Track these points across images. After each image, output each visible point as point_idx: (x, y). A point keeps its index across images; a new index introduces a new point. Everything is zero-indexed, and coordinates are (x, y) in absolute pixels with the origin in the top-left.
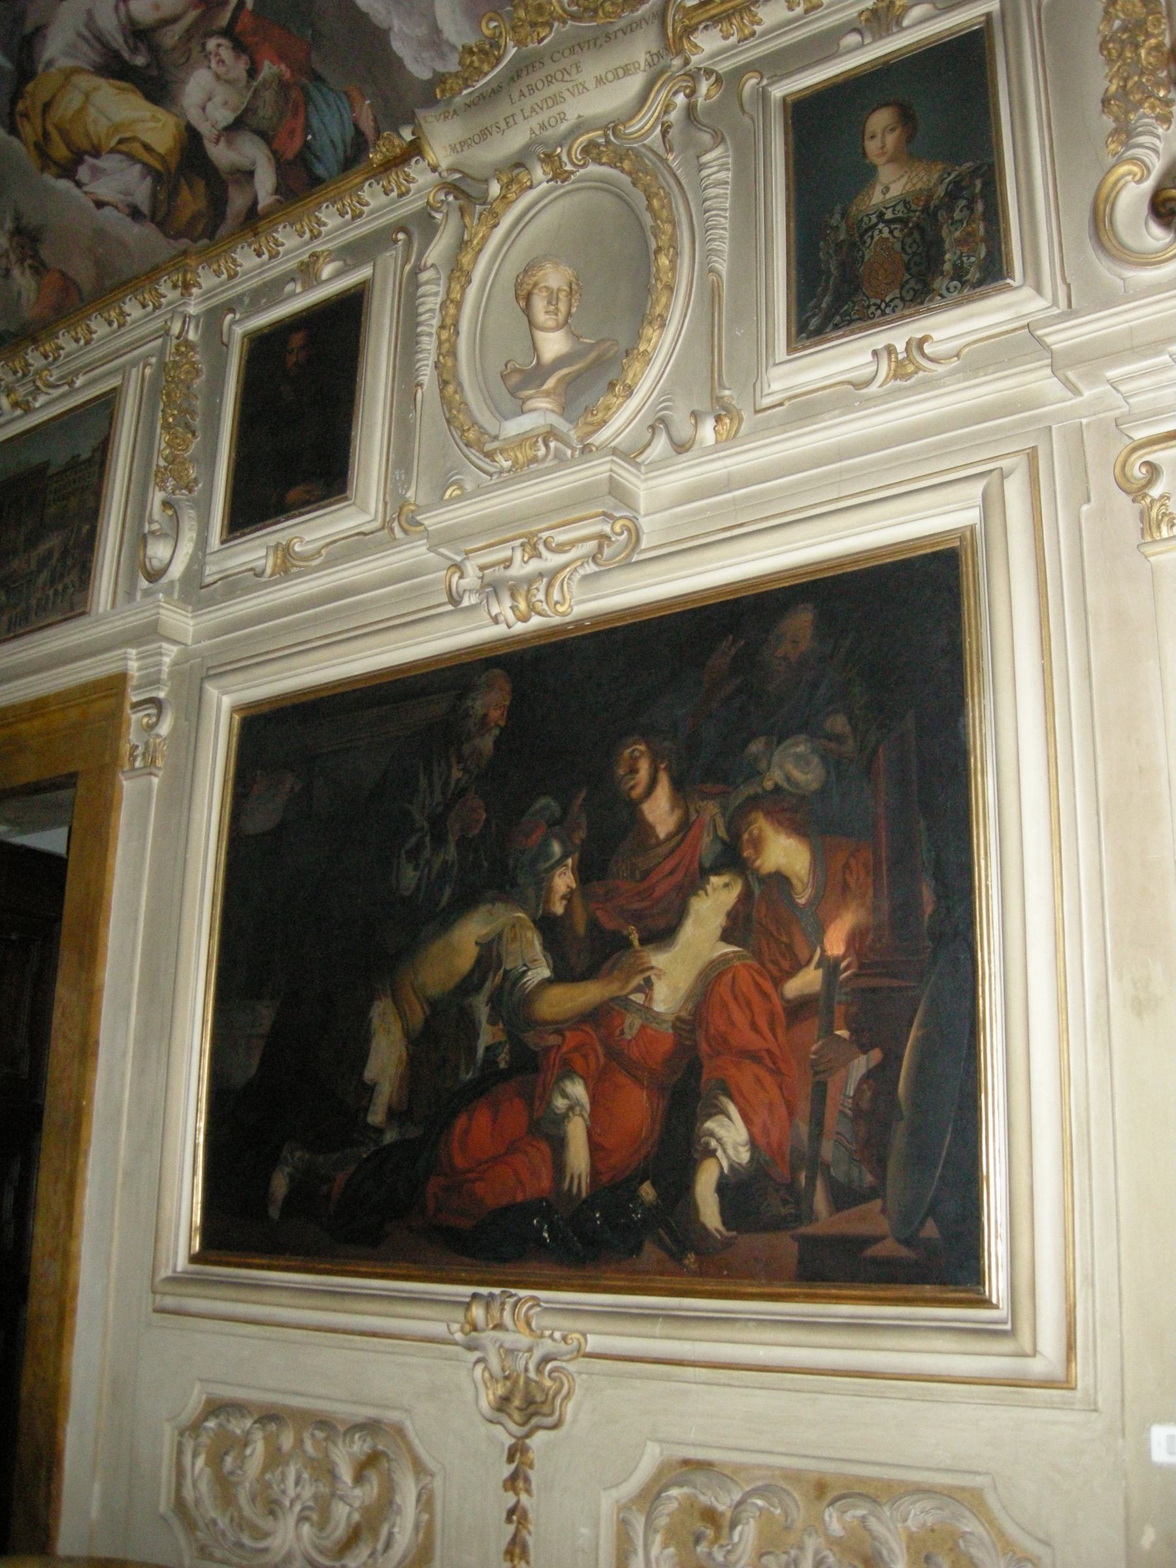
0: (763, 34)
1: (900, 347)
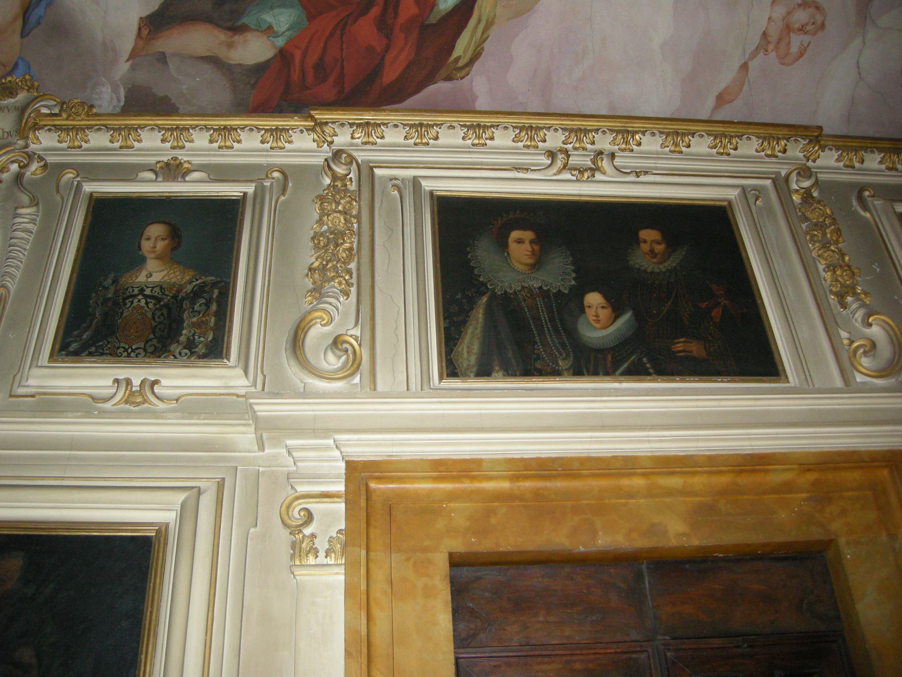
0: (86, 150)
1: (136, 382)
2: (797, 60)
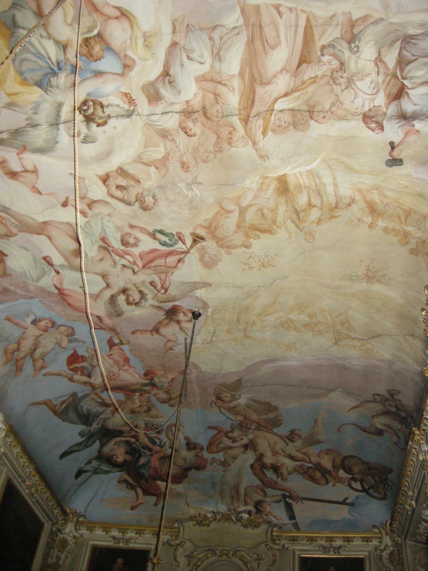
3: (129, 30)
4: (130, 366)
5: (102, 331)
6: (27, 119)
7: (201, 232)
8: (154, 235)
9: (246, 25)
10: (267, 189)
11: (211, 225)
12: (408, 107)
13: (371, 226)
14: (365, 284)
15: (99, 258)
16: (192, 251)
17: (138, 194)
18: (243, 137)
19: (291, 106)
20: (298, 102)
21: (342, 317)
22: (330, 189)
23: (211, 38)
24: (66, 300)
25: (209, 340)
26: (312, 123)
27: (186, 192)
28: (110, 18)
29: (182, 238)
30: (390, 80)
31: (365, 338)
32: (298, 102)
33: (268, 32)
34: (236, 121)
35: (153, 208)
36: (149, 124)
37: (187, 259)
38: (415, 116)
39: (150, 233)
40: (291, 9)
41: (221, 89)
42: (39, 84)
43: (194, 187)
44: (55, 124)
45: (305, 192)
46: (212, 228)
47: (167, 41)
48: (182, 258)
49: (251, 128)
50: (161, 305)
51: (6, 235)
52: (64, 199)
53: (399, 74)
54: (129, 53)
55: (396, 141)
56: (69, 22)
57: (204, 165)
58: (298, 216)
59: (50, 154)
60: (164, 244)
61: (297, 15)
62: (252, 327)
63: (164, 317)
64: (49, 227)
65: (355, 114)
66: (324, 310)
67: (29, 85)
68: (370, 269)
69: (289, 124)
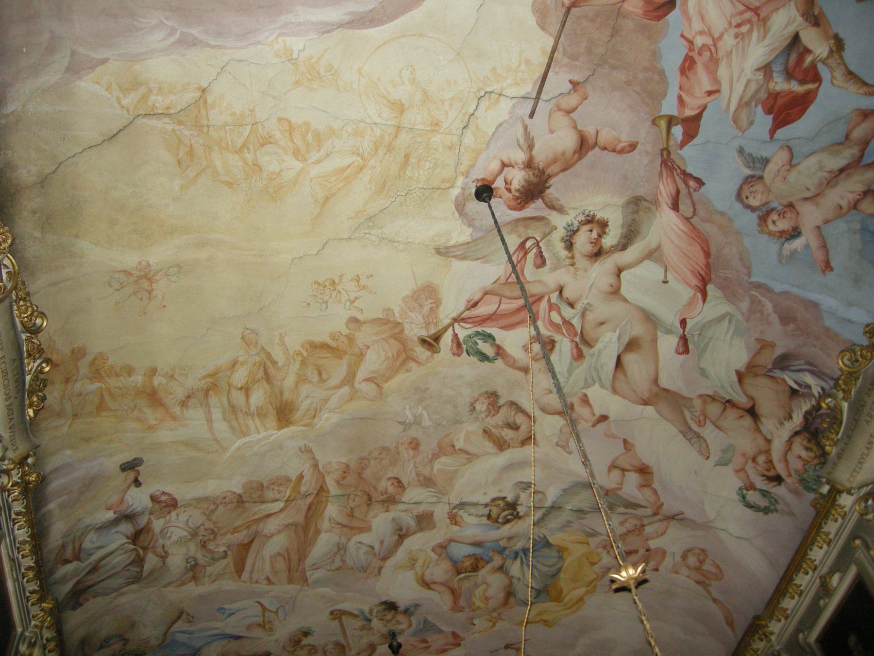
2: (721, 571)
3: (427, 573)
4: (691, 42)
5: (689, 170)
6: (583, 519)
7: (421, 352)
8: (497, 354)
9: (304, 571)
10: (308, 410)
11: (404, 362)
12: (126, 528)
13: (153, 371)
14: (153, 261)
15: (604, 328)
16: (447, 321)
17: (494, 415)
18: (329, 473)
19: (264, 506)
20: (256, 509)
21: (191, 173)
22: (217, 414)
23: (344, 561)
24: (708, 265)
25: (484, 104)
26: (239, 491)
27: (424, 413)
28: (441, 584)
29: (455, 345)
30: (149, 544)
31: (140, 121)
32: (256, 509)
33: (281, 565)
34: (333, 489)
35: (481, 395)
36: (441, 494)
37: (462, 307)
38: (115, 522)
39: (503, 358)
40: (257, 582)
41: (344, 520)
42: (548, 545)
43: (410, 418)
44: (555, 508)
45: (253, 408)
46: (403, 356)
47: (391, 562)
48: (468, 309)
49: (317, 482)
50: (546, 212)
51: (714, 399)
52: (602, 426)
53: (141, 552)
54: (434, 556)
55: (133, 490)
56: (484, 586)
57: (387, 445)
58: (266, 373)
59: (581, 480)
60: (489, 337)
61: (251, 578)
62: (382, 137)
63: (552, 181)
64: (646, 395)
65: (187, 505)
66: (229, 184)
67: (559, 546)
68: (147, 294)
69: (268, 488)
